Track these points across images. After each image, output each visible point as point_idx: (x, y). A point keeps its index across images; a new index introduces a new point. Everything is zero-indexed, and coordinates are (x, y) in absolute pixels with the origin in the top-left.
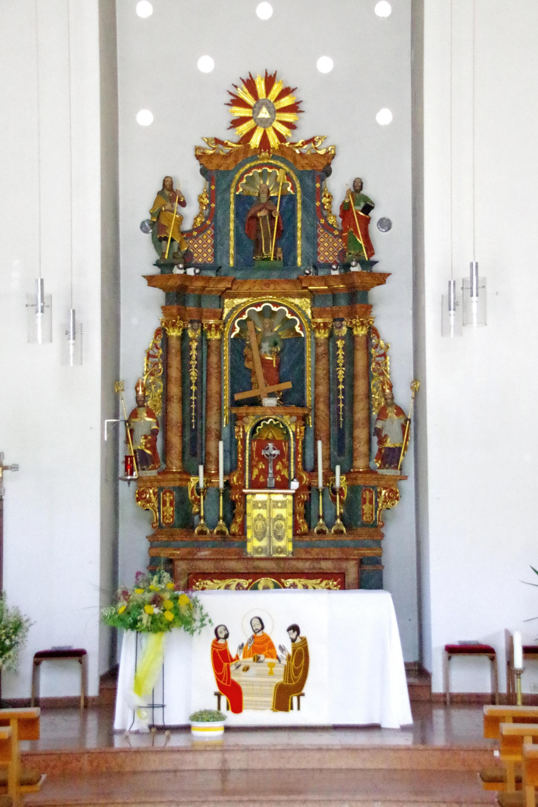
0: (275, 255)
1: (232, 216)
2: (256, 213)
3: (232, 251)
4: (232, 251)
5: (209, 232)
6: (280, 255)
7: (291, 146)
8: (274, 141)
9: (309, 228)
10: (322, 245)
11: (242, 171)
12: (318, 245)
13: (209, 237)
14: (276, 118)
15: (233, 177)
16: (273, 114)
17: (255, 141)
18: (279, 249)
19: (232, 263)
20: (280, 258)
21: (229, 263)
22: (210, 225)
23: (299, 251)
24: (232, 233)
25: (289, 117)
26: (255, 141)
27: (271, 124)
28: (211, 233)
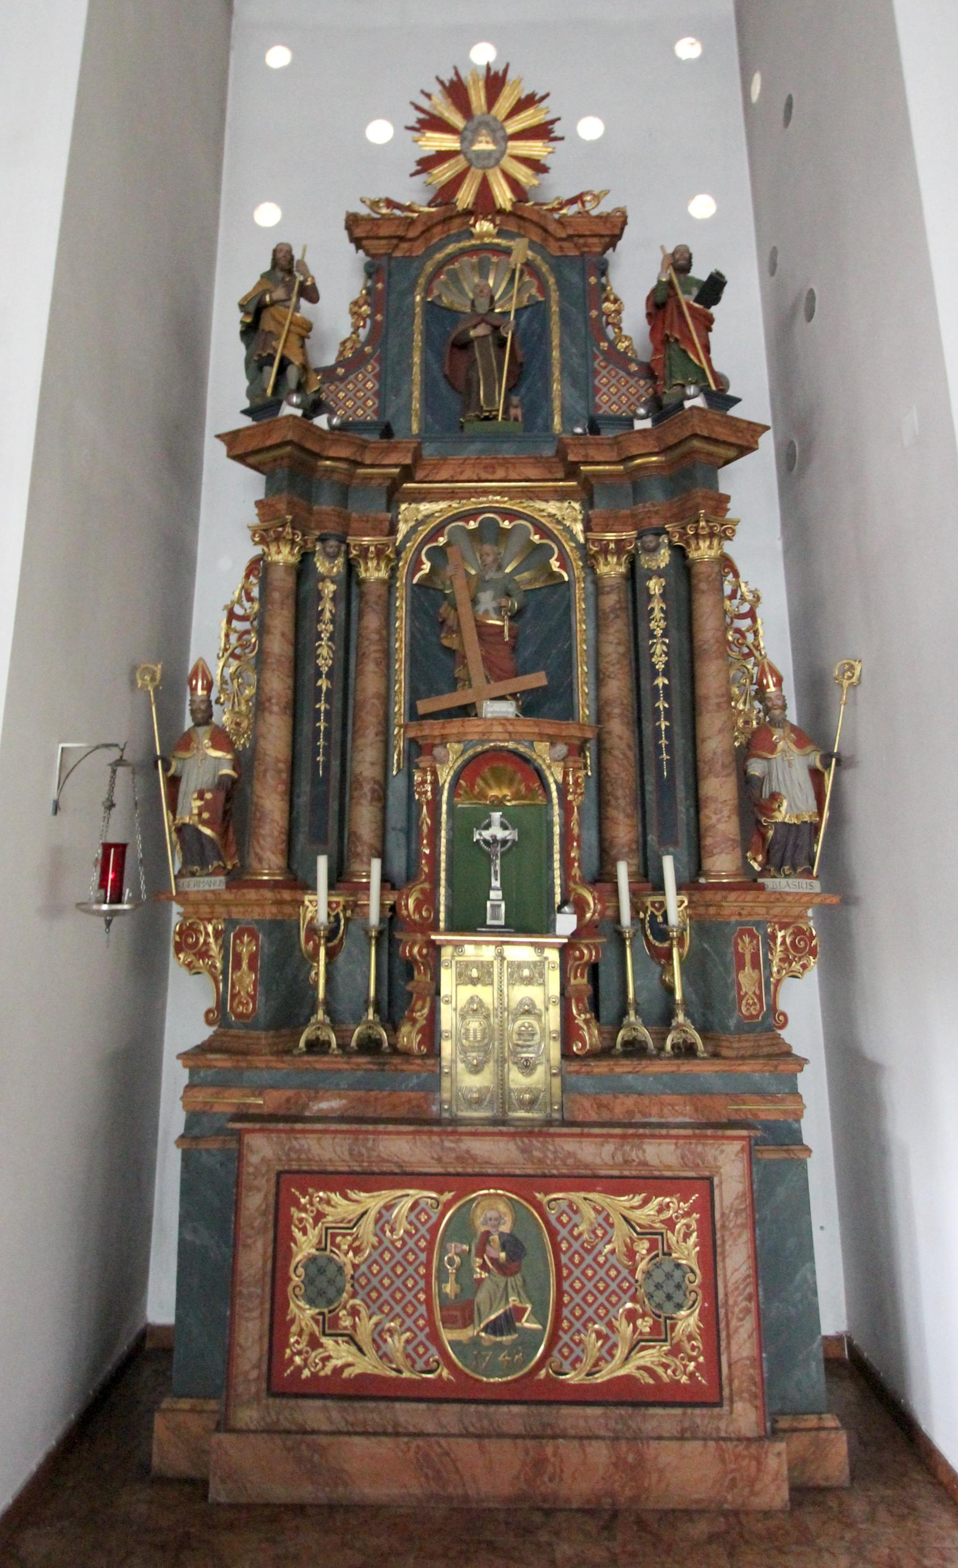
0: (506, 411)
1: (418, 338)
2: (466, 332)
3: (416, 405)
4: (416, 405)
5: (370, 368)
6: (516, 412)
7: (536, 208)
8: (503, 196)
9: (575, 359)
10: (604, 390)
11: (439, 256)
12: (597, 390)
13: (369, 376)
14: (508, 151)
15: (422, 268)
16: (503, 143)
17: (465, 197)
18: (515, 400)
19: (415, 428)
20: (516, 419)
21: (410, 429)
22: (371, 356)
23: (557, 404)
24: (416, 370)
25: (534, 149)
26: (465, 197)
27: (497, 162)
28: (374, 369)
